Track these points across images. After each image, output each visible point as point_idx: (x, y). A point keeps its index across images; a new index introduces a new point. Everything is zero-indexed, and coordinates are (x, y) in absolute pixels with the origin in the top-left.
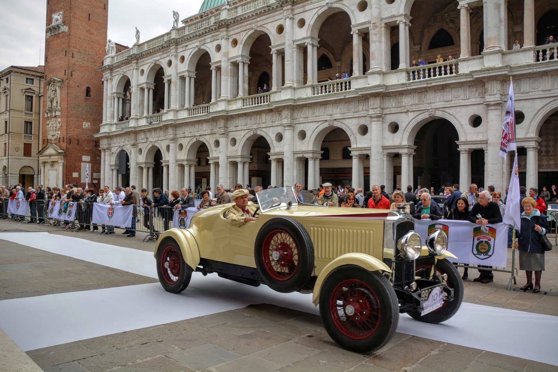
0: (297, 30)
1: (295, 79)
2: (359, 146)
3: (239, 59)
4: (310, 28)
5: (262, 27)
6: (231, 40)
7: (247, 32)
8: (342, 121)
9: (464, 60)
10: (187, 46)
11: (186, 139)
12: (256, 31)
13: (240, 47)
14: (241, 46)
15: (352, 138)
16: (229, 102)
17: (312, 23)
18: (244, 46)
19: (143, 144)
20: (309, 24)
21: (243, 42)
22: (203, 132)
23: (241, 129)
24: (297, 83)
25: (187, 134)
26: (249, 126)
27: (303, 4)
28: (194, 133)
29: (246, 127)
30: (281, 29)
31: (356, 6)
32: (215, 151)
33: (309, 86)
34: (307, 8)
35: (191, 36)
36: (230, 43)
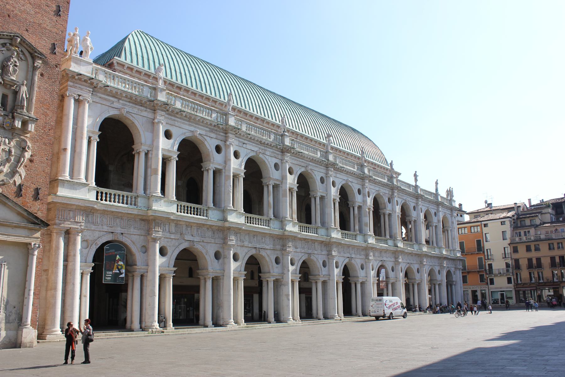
5: (312, 171)
7: (300, 167)
10: (244, 143)
11: (244, 248)
15: (358, 271)
19: (170, 240)
22: (265, 246)
23: (299, 251)
25: (246, 244)
26: (306, 250)
27: (336, 172)
28: (255, 244)
29: (303, 250)
32: (277, 267)
34: (338, 176)
35: (256, 139)
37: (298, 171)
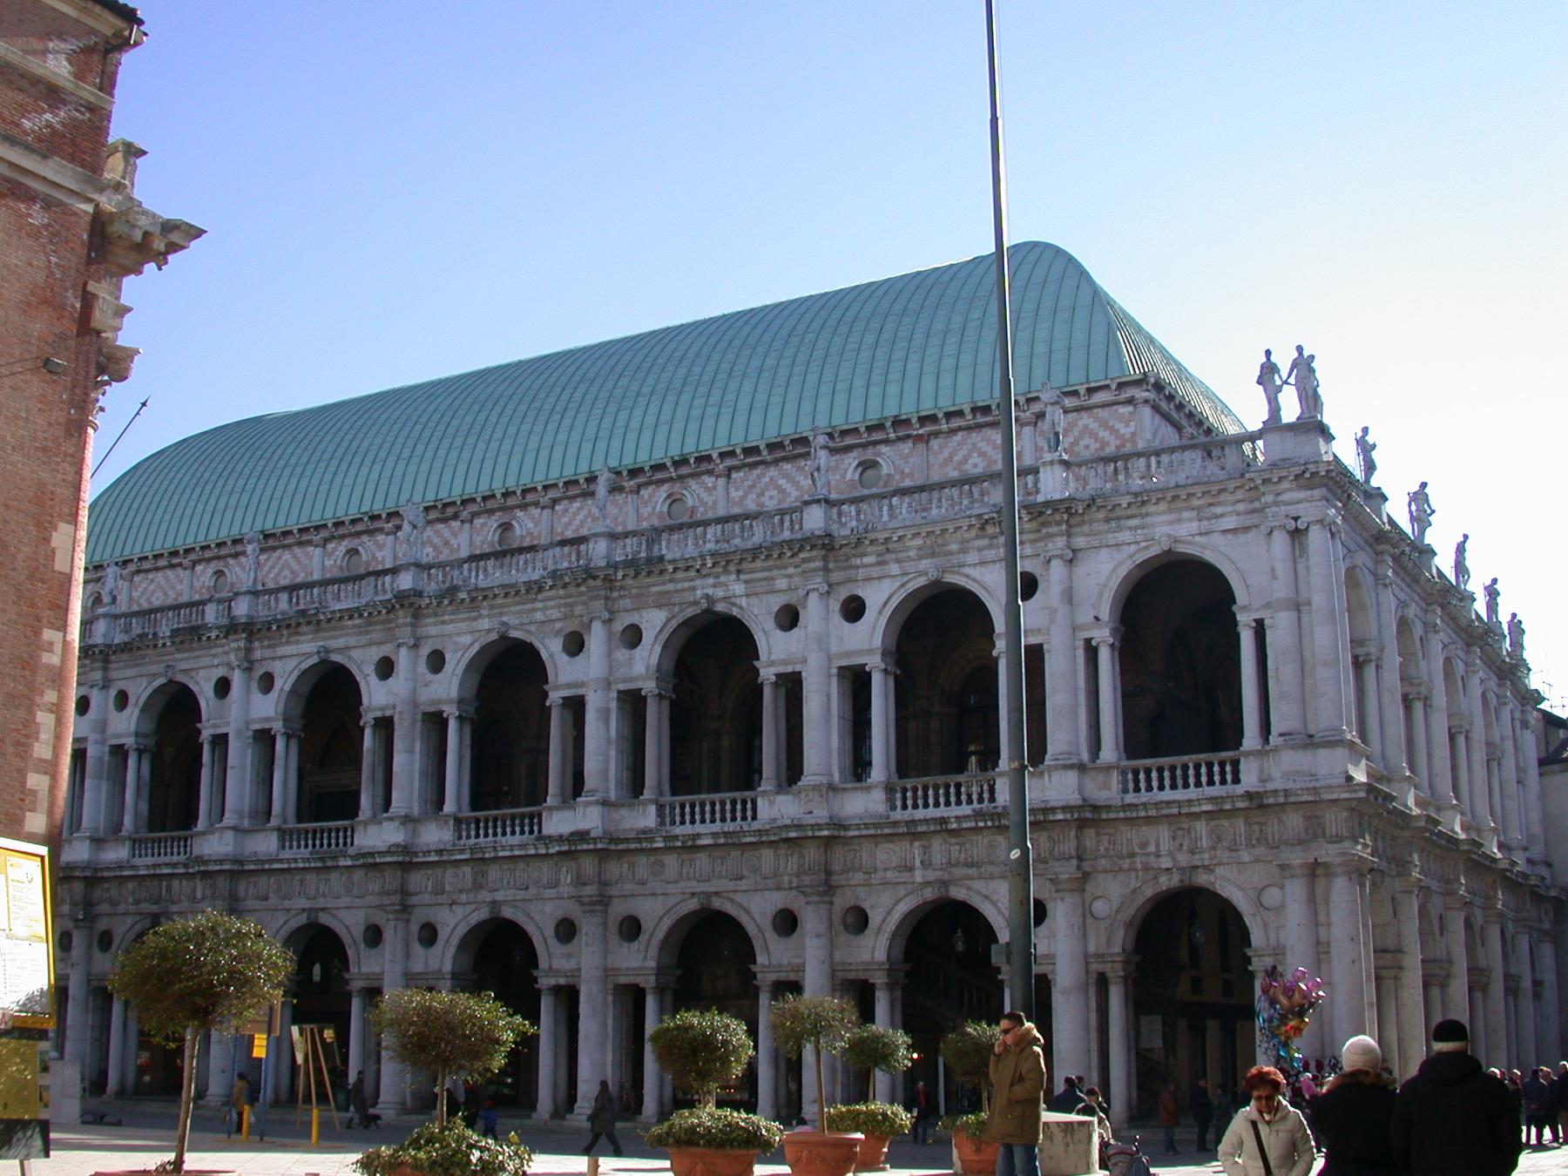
0: (257, 696)
1: (247, 808)
2: (365, 970)
3: (130, 741)
4: (284, 697)
6: (113, 692)
8: (335, 912)
9: (550, 809)
12: (171, 681)
13: (132, 712)
14: (137, 712)
16: (98, 841)
17: (287, 687)
18: (142, 710)
20: (282, 689)
21: (142, 701)
24: (251, 818)
30: (223, 687)
31: (373, 667)
33: (273, 829)
36: (112, 699)
37: (140, 691)
